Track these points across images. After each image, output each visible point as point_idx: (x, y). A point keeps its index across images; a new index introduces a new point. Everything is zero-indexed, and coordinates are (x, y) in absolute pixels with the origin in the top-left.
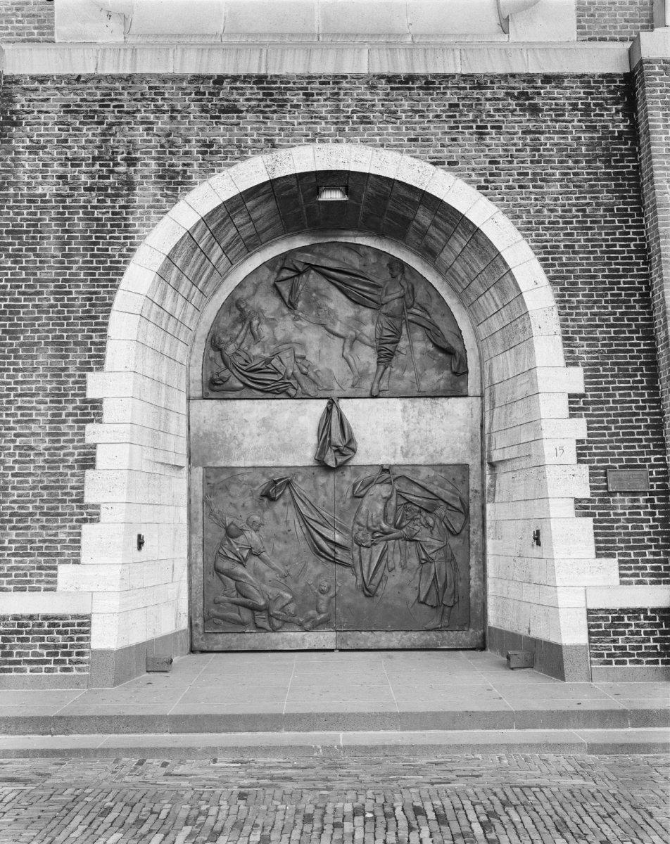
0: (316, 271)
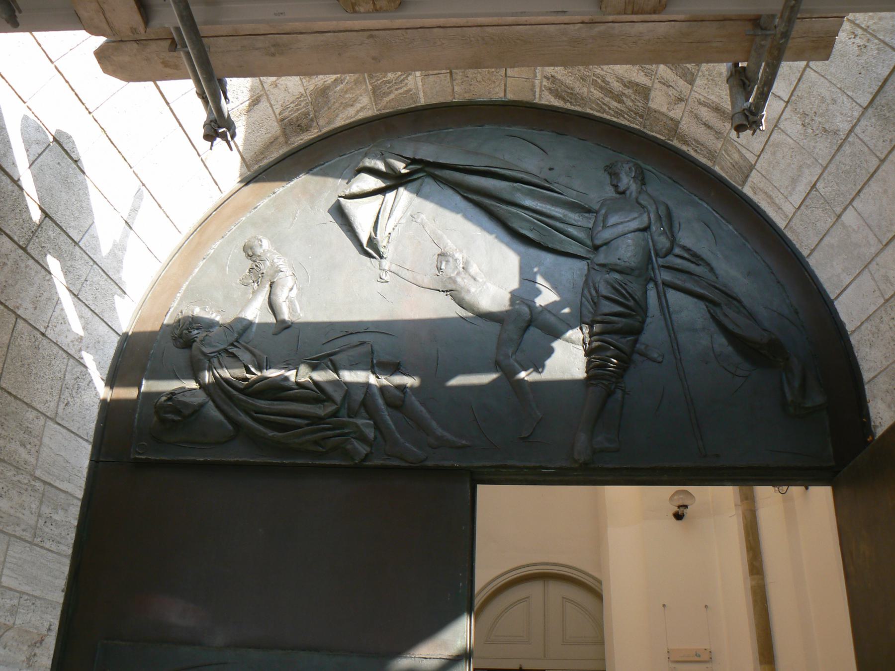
0: (436, 178)
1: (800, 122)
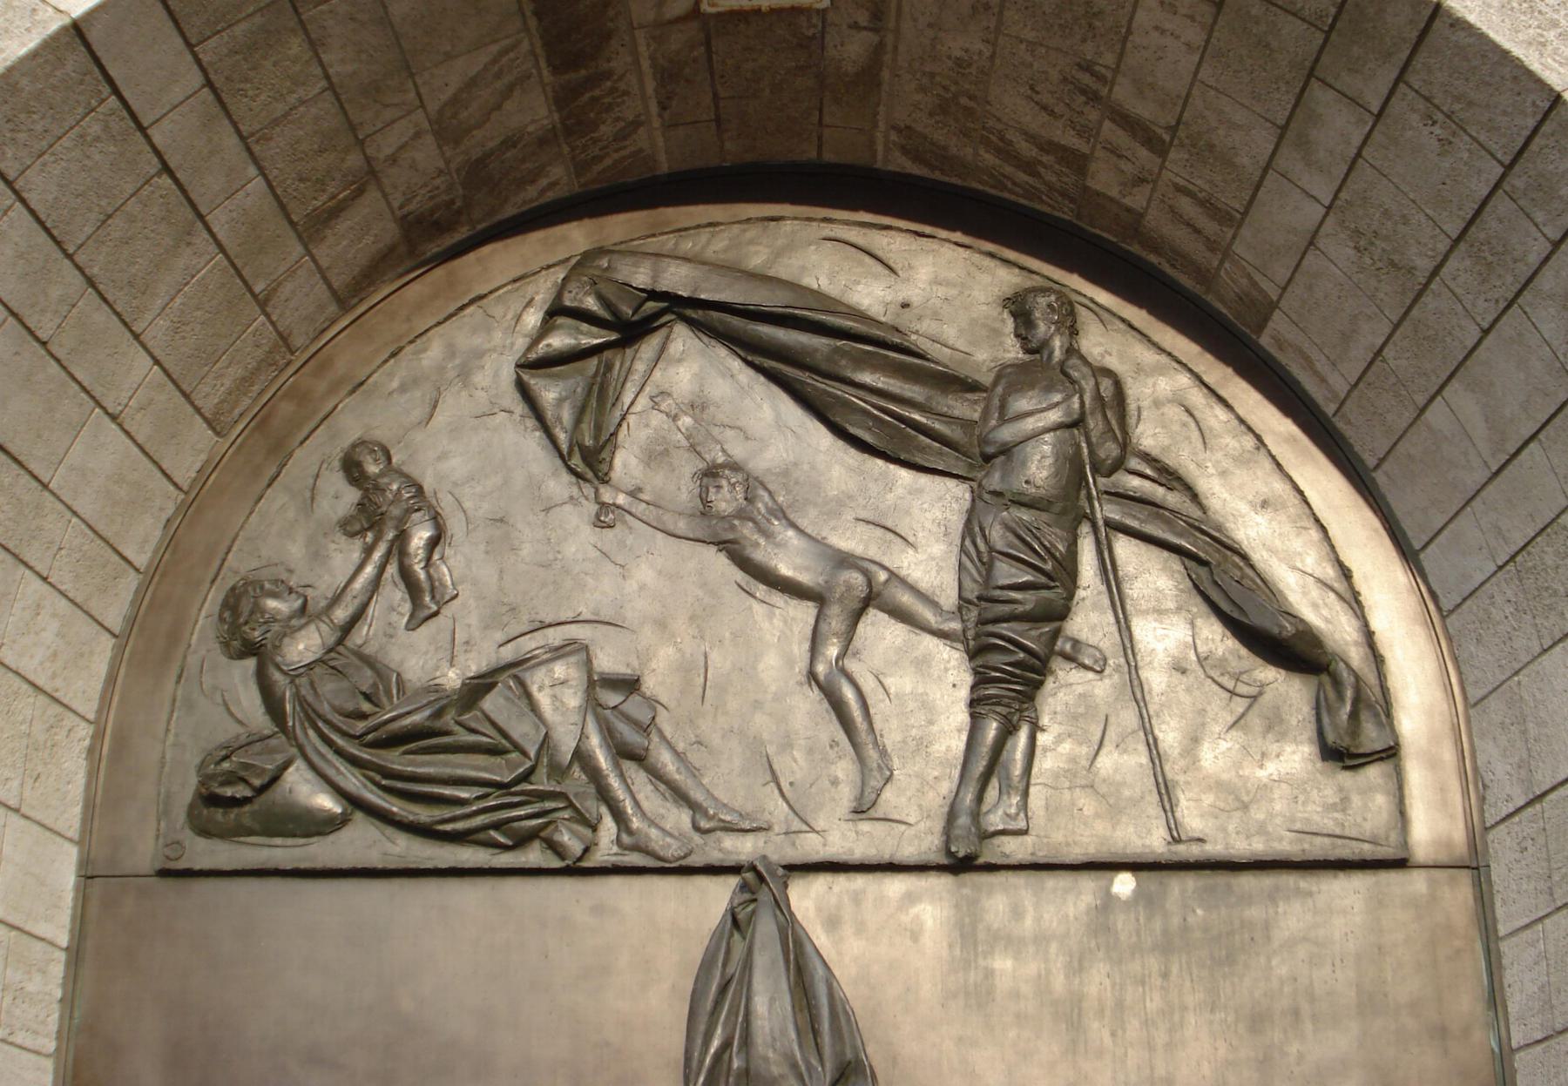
0: (693, 324)
1: (1352, 244)
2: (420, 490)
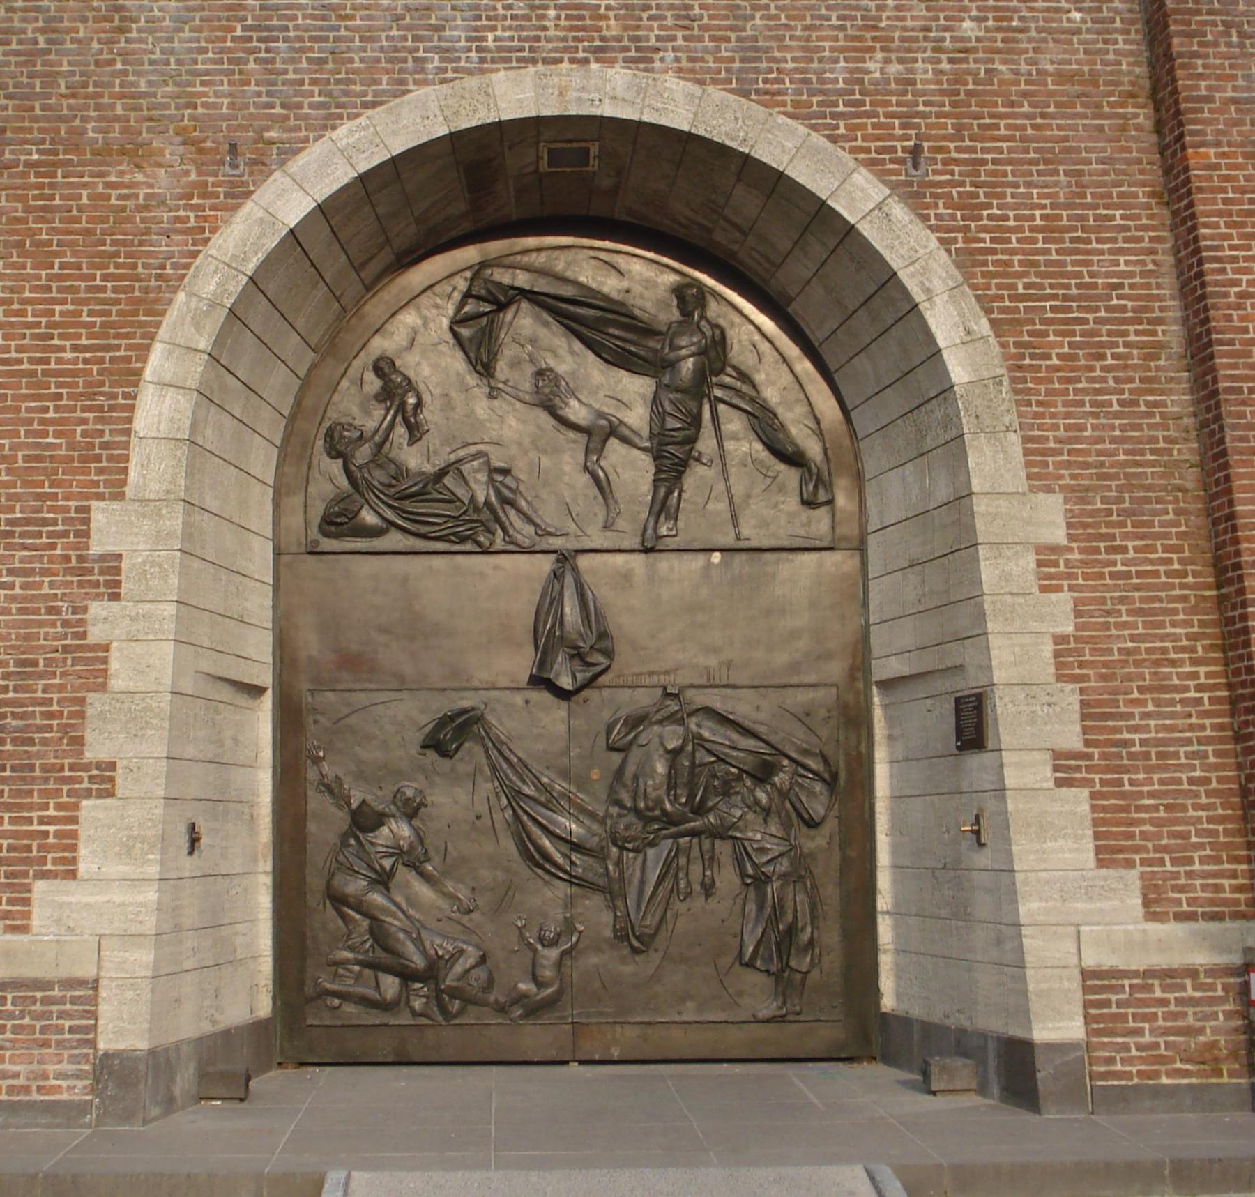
0: (530, 300)
2: (410, 381)
